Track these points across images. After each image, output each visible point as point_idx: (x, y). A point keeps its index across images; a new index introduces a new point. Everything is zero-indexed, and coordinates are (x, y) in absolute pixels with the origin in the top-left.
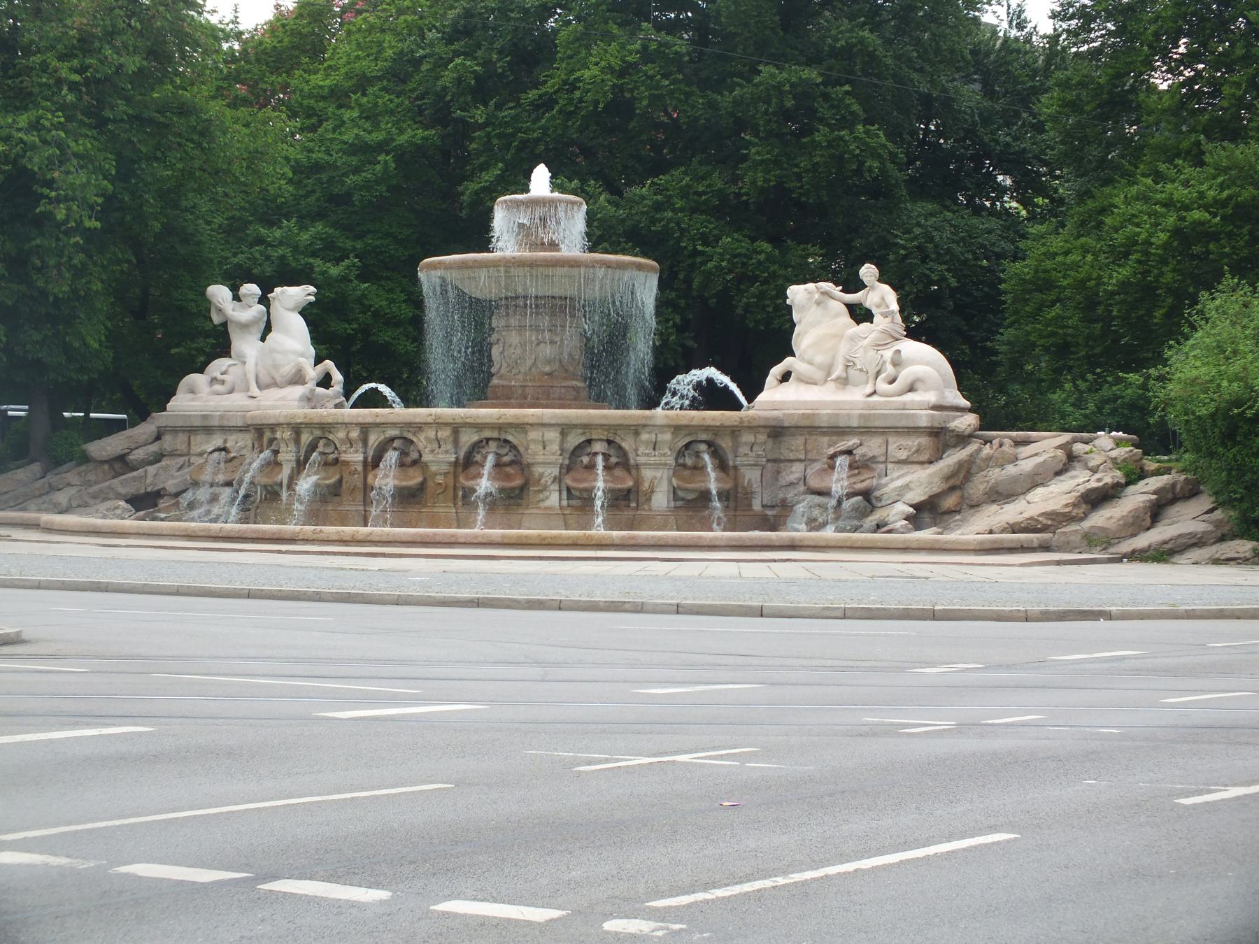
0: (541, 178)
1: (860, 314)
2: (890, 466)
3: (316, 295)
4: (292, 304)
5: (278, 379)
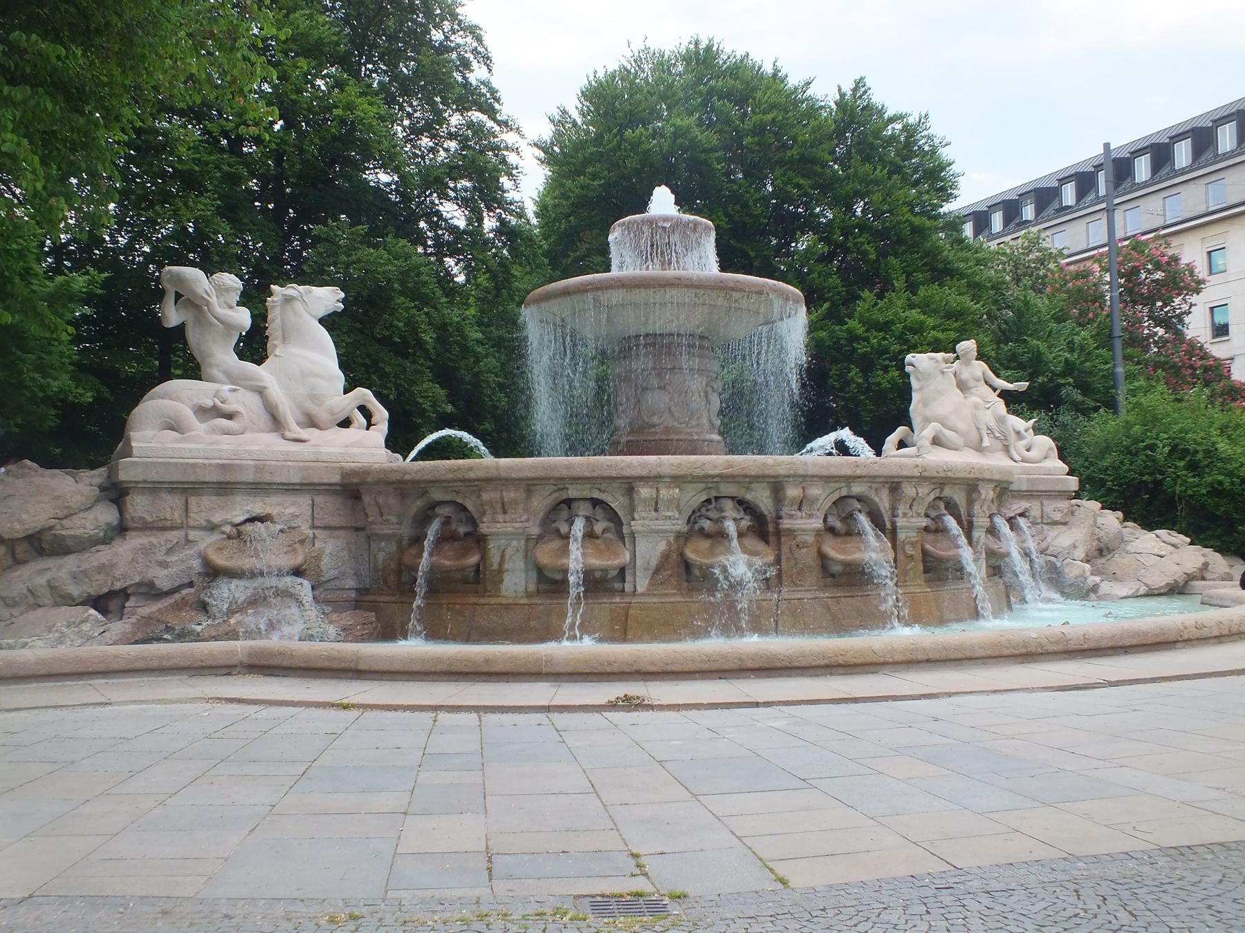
0: (662, 201)
1: (963, 386)
2: (1045, 527)
3: (344, 301)
4: (322, 313)
5: (322, 415)
